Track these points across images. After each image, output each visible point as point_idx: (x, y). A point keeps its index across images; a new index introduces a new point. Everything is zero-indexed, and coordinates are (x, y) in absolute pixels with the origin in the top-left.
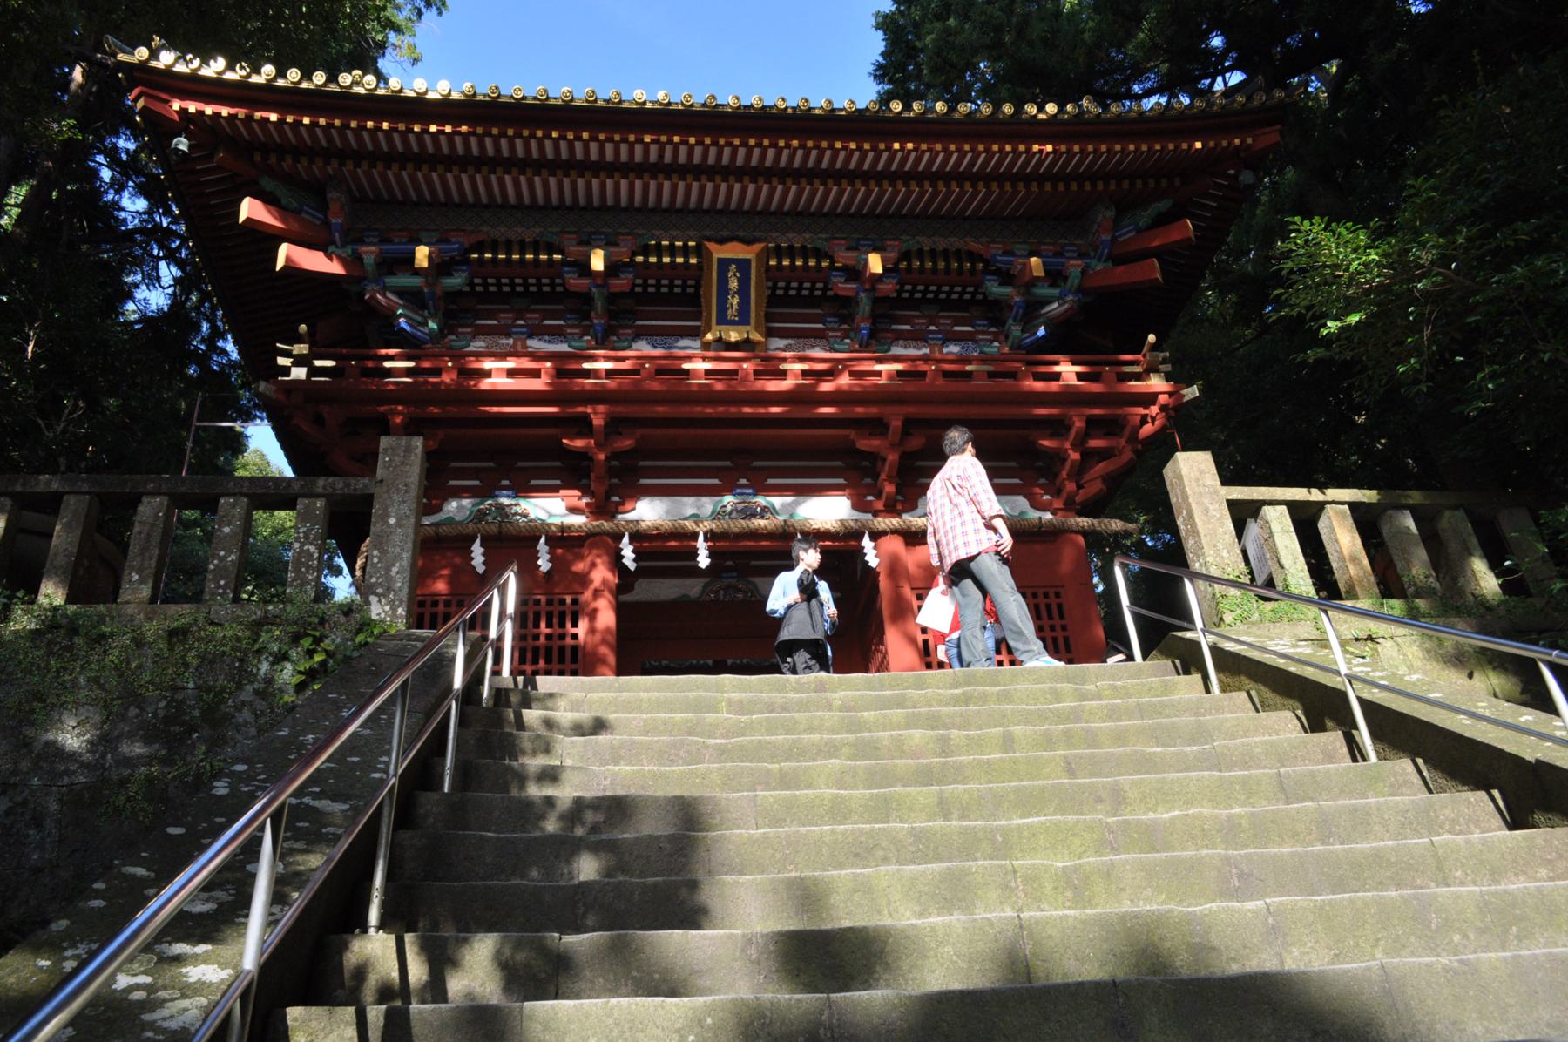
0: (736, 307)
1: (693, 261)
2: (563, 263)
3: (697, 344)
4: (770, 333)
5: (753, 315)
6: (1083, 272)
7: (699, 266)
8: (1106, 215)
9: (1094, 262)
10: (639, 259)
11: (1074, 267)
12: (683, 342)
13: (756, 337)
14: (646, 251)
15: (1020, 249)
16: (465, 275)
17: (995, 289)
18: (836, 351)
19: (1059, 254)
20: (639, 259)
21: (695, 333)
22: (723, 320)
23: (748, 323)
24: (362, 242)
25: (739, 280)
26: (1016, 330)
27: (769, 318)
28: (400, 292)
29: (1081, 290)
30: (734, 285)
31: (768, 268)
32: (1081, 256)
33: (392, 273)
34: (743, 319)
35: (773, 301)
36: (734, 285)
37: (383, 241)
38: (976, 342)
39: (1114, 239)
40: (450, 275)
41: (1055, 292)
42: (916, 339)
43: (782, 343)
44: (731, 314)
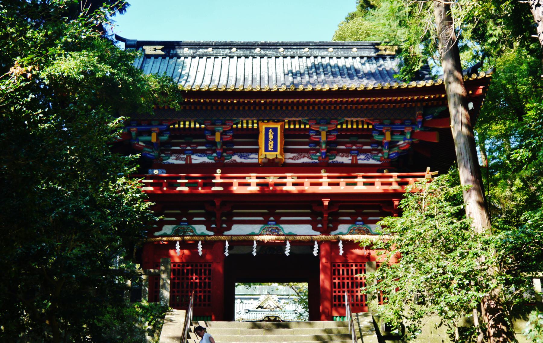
0: (272, 145)
3: (256, 156)
16: (168, 135)
18: (313, 159)
28: (144, 142)
30: (271, 136)
36: (271, 136)
37: (139, 124)
38: (372, 154)
40: (163, 136)
42: (347, 153)
44: (271, 148)
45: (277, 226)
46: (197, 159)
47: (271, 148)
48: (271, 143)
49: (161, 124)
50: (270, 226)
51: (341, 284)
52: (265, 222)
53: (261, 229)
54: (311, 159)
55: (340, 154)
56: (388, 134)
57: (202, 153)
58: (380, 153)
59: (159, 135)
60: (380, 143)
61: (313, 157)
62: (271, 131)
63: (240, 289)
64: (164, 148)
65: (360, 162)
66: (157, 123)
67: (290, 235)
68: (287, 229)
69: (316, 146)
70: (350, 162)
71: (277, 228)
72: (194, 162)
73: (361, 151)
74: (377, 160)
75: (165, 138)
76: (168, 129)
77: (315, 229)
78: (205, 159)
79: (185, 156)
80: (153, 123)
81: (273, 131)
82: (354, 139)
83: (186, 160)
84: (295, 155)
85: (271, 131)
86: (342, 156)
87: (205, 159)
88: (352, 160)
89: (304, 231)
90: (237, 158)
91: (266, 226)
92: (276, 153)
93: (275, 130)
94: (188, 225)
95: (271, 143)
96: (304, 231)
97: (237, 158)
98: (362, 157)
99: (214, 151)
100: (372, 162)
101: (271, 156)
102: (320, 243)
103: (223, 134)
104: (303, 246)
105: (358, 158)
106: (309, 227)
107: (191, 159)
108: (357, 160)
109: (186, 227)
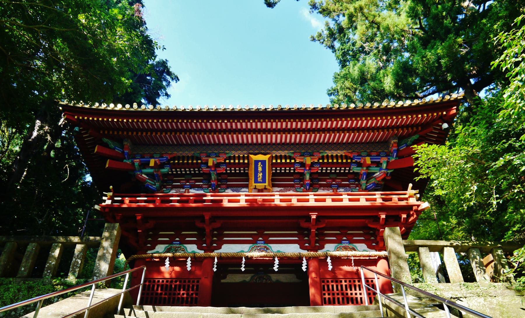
22: (256, 181)
28: (147, 174)
30: (260, 169)
36: (260, 169)
40: (164, 168)
44: (260, 179)
45: (265, 245)
47: (260, 179)
50: (259, 245)
53: (250, 248)
62: (260, 163)
66: (158, 156)
67: (278, 251)
68: (276, 248)
77: (302, 247)
81: (262, 164)
84: (282, 189)
85: (260, 163)
89: (292, 250)
92: (265, 184)
96: (292, 250)
102: (308, 259)
104: (291, 264)
105: (338, 191)
106: (297, 246)
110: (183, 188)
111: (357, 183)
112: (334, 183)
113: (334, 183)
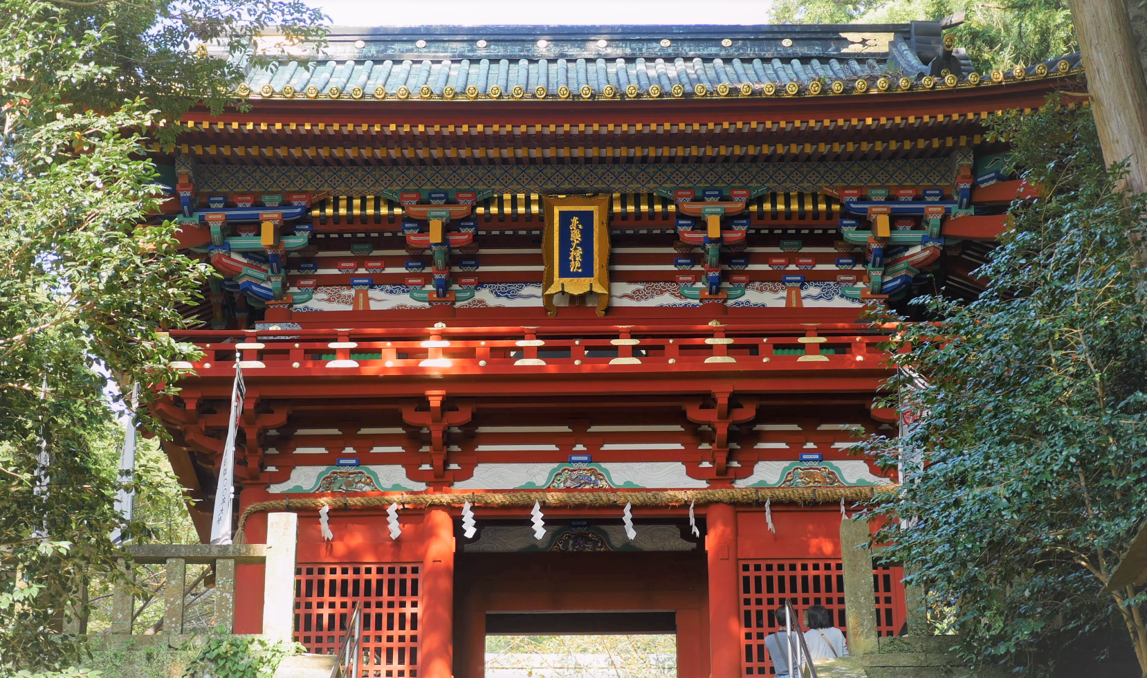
1: (535, 209)
2: (406, 219)
3: (538, 291)
4: (614, 277)
5: (596, 266)
6: (944, 219)
7: (540, 218)
8: (964, 162)
9: (954, 208)
10: (480, 210)
11: (934, 213)
12: (528, 290)
13: (599, 289)
14: (486, 203)
15: (879, 194)
16: (306, 234)
17: (851, 234)
19: (918, 199)
20: (480, 210)
21: (534, 279)
22: (565, 272)
23: (592, 276)
24: (206, 207)
25: (582, 232)
26: (876, 275)
27: (613, 259)
28: (245, 254)
29: (941, 235)
30: (576, 236)
31: (612, 217)
32: (945, 199)
33: (236, 234)
34: (587, 271)
35: (615, 241)
36: (576, 236)
37: (229, 206)
39: (974, 186)
41: (917, 235)
43: (629, 288)
44: (575, 265)
45: (592, 466)
46: (383, 300)
47: (575, 265)
48: (576, 254)
49: (286, 204)
50: (575, 466)
51: (755, 650)
52: (561, 457)
53: (551, 474)
54: (682, 296)
55: (757, 284)
56: (883, 229)
57: (397, 283)
58: (859, 279)
59: (284, 230)
60: (859, 255)
61: (686, 292)
62: (575, 220)
63: (490, 640)
64: (295, 267)
65: (808, 303)
66: (278, 199)
68: (620, 474)
69: (693, 264)
70: (782, 304)
71: (593, 472)
72: (374, 306)
73: (808, 278)
74: (853, 299)
75: (299, 240)
76: (304, 219)
77: (693, 472)
78: (404, 300)
79: (353, 292)
80: (266, 199)
81: (581, 221)
82: (790, 247)
83: (356, 299)
84: (640, 286)
85: (575, 220)
86: (762, 290)
87: (404, 300)
88: (788, 299)
90: (487, 297)
91: (566, 466)
92: (587, 280)
93: (586, 218)
94: (357, 465)
95: (576, 254)
97: (487, 297)
98: (814, 290)
99: (428, 279)
100: (838, 303)
101: (577, 287)
103: (450, 227)
105: (803, 293)
106: (679, 467)
107: (367, 299)
108: (800, 299)
109: (352, 470)
110: (350, 286)
111: (859, 267)
112: (792, 267)
113: (792, 267)
